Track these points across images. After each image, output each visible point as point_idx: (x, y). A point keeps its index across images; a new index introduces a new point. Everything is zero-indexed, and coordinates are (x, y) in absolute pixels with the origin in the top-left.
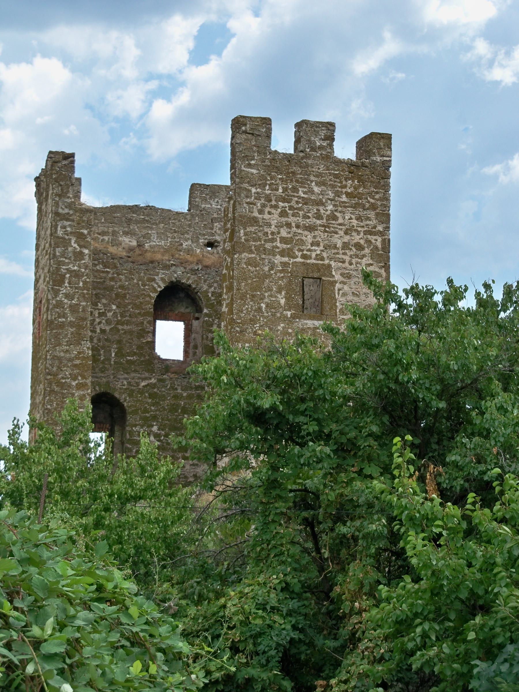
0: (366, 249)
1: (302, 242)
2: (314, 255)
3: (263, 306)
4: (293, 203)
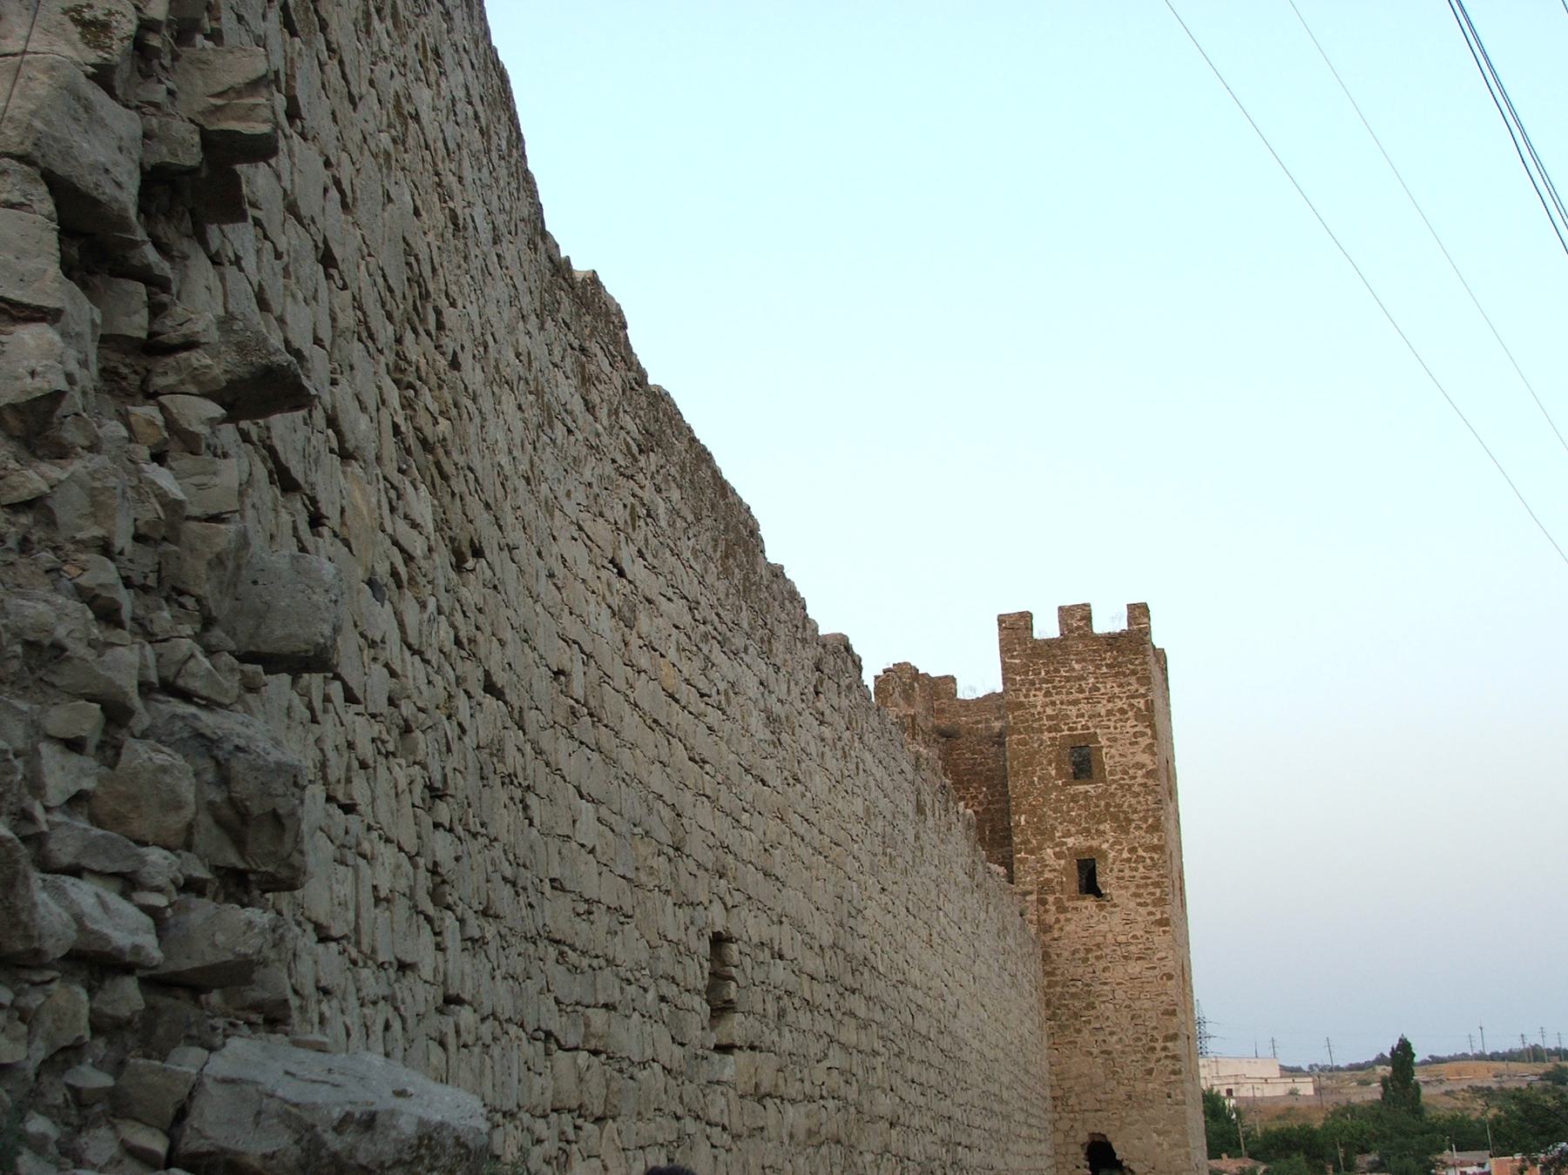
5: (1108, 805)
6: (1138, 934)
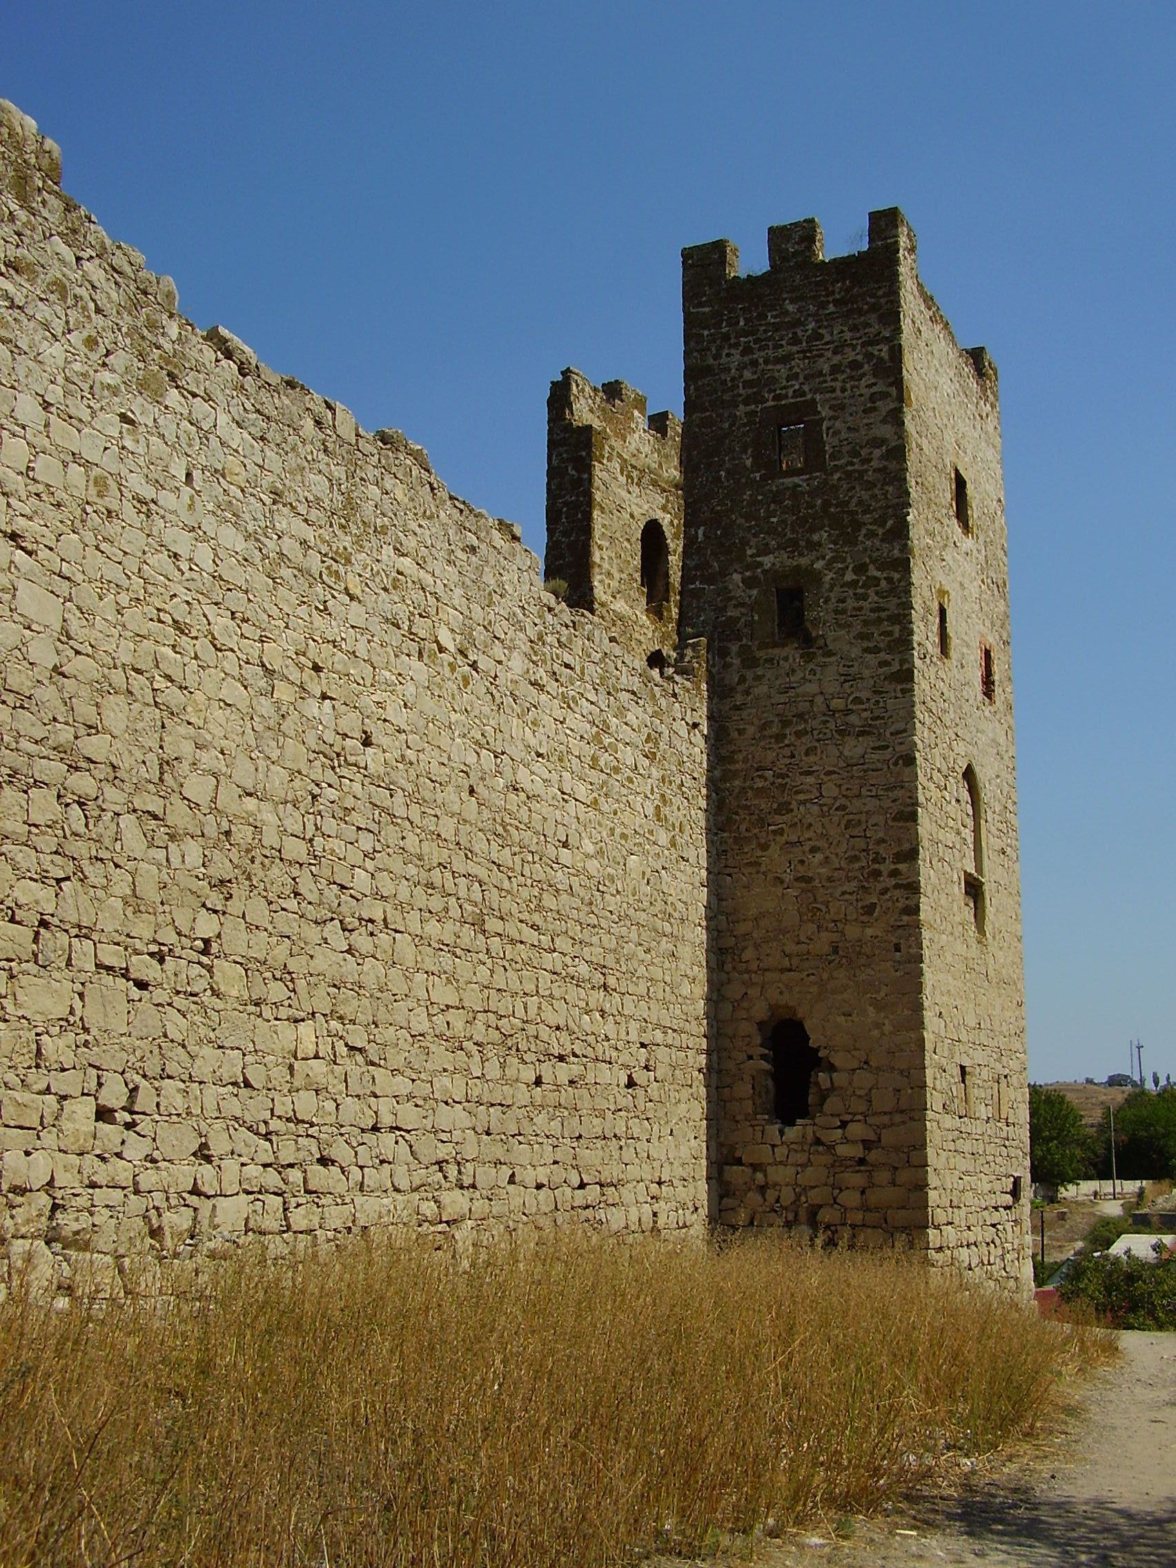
0: (866, 366)
1: (774, 380)
2: (790, 394)
3: (723, 473)
4: (760, 335)
5: (827, 504)
6: (864, 695)
